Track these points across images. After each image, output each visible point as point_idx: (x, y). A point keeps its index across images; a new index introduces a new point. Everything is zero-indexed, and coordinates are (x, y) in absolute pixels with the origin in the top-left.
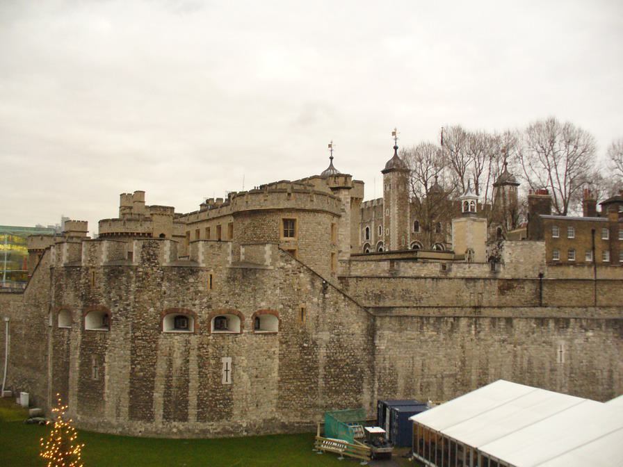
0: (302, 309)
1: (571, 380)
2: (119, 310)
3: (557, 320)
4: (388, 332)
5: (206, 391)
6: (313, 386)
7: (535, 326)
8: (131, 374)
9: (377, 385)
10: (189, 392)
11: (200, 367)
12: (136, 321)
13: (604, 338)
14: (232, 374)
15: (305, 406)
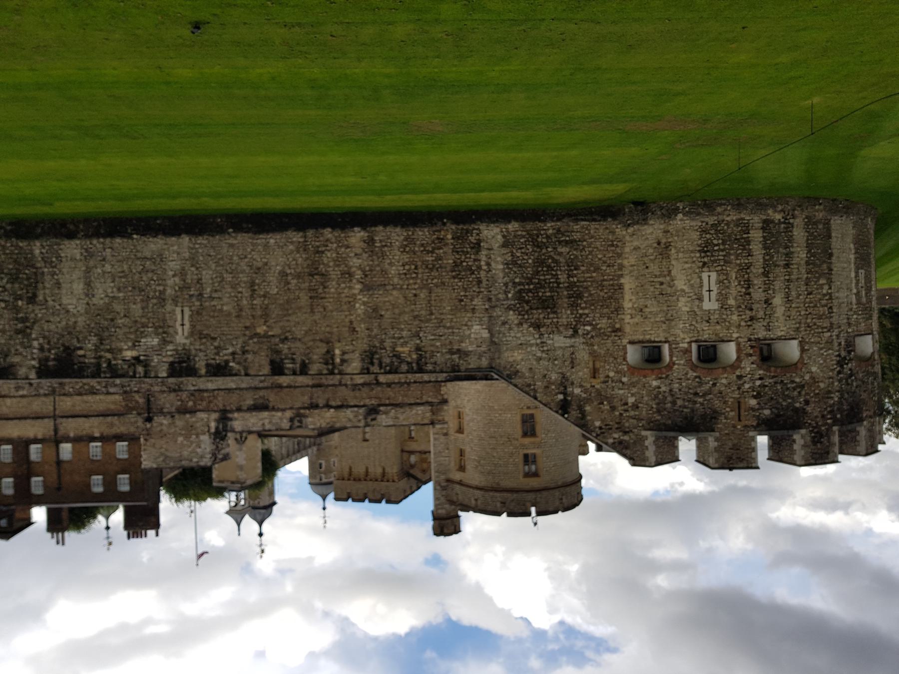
0: (594, 377)
1: (165, 280)
2: (847, 364)
3: (192, 372)
4: (470, 349)
5: (738, 262)
6: (575, 272)
7: (231, 364)
8: (831, 282)
9: (483, 274)
10: (762, 260)
11: (749, 294)
12: (831, 351)
13: (102, 347)
14: (701, 286)
15: (585, 243)
